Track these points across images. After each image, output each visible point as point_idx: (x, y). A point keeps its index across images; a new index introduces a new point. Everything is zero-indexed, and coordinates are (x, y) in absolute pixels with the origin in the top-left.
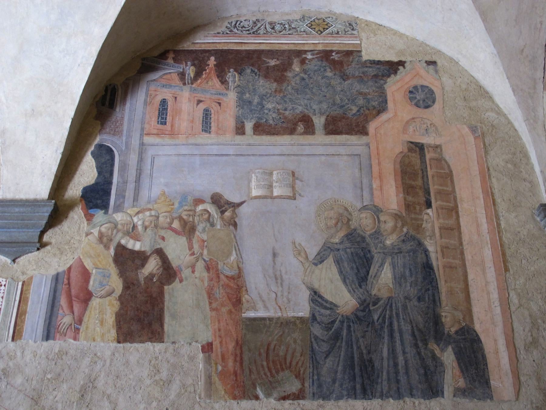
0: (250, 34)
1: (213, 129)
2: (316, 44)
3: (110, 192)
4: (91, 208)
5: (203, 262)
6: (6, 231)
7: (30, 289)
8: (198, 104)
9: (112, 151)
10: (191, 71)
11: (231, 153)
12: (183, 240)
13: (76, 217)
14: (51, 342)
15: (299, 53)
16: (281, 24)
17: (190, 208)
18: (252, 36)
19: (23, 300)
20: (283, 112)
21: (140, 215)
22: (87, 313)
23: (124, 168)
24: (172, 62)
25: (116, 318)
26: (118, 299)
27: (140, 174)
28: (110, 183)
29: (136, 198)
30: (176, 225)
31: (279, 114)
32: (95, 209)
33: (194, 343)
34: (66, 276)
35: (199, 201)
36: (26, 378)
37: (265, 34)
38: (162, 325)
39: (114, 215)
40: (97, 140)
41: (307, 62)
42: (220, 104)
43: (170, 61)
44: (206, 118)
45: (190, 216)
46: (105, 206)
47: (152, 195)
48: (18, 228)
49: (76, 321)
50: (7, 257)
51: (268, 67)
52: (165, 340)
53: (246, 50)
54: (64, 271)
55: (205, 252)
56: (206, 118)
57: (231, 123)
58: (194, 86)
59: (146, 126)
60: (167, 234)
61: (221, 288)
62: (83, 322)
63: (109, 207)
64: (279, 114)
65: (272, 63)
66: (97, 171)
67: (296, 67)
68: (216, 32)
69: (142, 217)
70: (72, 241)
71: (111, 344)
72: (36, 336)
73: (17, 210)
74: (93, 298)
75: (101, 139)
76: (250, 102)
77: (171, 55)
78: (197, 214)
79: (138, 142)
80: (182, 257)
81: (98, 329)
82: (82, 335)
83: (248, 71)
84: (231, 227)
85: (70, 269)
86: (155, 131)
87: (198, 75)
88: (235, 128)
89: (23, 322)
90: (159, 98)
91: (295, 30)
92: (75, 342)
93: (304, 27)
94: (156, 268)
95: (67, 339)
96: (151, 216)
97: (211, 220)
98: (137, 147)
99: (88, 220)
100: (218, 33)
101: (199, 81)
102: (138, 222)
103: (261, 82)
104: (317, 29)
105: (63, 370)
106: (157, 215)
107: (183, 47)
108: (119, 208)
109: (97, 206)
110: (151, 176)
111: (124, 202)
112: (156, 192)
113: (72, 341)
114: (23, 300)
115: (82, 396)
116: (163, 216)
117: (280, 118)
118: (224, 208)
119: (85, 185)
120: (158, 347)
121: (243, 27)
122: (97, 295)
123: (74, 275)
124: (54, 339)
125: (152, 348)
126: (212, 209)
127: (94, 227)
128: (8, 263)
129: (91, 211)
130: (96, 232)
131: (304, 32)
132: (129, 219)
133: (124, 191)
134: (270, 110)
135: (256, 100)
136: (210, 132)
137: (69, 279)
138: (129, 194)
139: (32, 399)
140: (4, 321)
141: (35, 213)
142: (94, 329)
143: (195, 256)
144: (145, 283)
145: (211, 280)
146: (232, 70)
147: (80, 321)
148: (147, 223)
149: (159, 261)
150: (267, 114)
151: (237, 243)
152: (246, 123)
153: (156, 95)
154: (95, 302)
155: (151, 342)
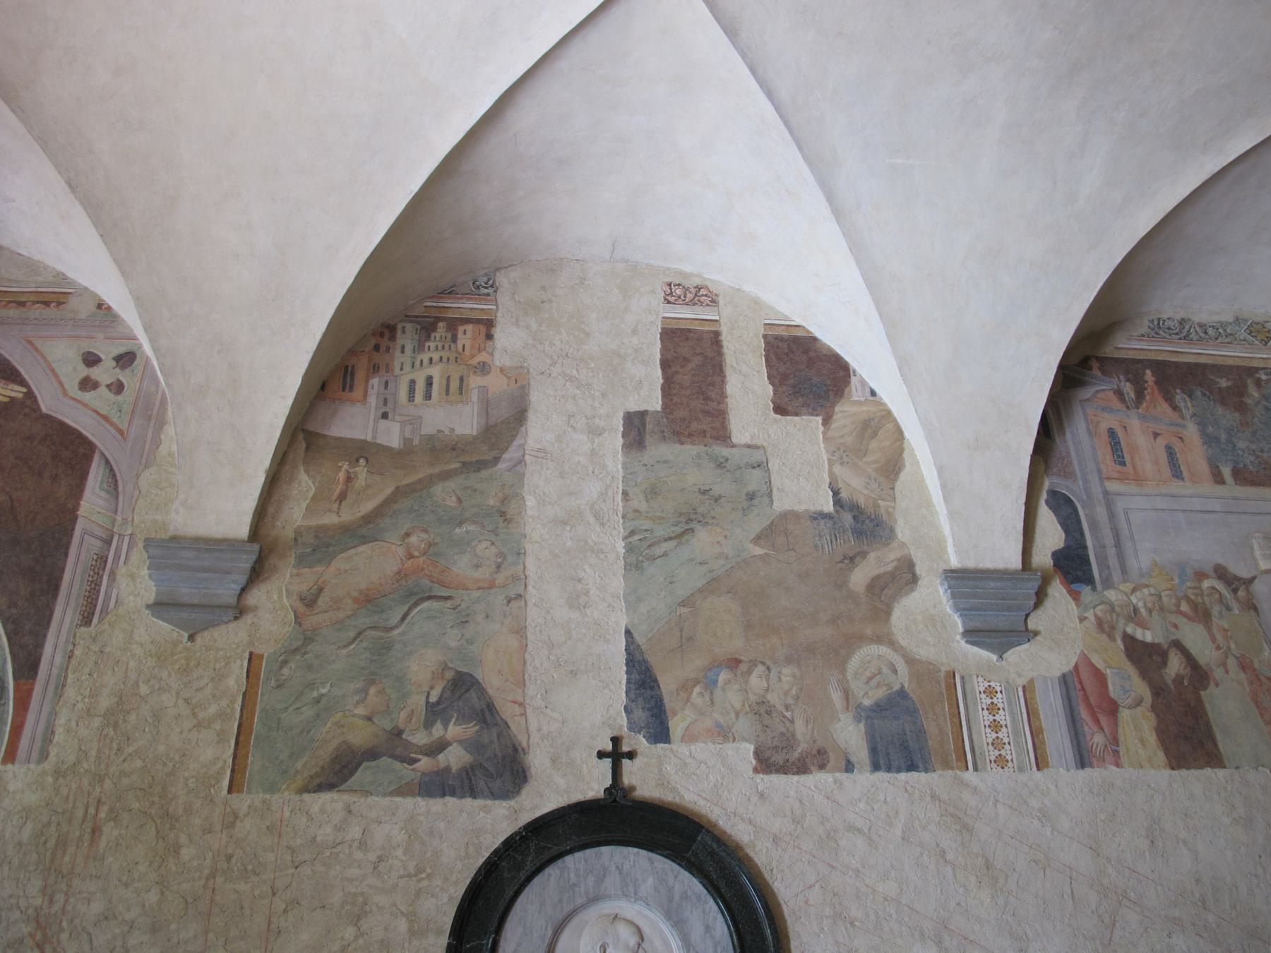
0: (1180, 339)
1: (1185, 474)
2: (1266, 359)
3: (1089, 559)
4: (1072, 583)
5: (1234, 658)
6: (979, 615)
7: (1036, 697)
8: (1155, 438)
9: (1071, 501)
10: (1128, 389)
11: (1218, 510)
12: (1200, 629)
13: (1057, 594)
14: (1088, 770)
15: (1251, 371)
16: (1213, 327)
17: (1193, 585)
18: (1184, 343)
19: (1032, 713)
20: (1260, 454)
21: (1138, 593)
22: (1120, 729)
23: (1094, 526)
24: (1099, 374)
25: (1157, 735)
26: (1150, 709)
27: (1117, 535)
28: (1085, 547)
29: (1124, 570)
30: (1184, 607)
31: (1257, 457)
32: (1079, 584)
33: (1260, 768)
34: (1075, 679)
35: (1200, 575)
36: (1074, 821)
37: (1198, 340)
38: (1215, 745)
39: (1105, 593)
40: (1047, 484)
41: (1263, 384)
42: (1181, 438)
43: (1096, 372)
44: (1172, 459)
45: (1197, 595)
46: (1089, 580)
47: (1142, 566)
48: (998, 611)
49: (1111, 741)
50: (991, 652)
51: (1220, 389)
52: (1227, 766)
53: (1184, 363)
54: (1070, 671)
55: (1233, 646)
56: (1172, 459)
57: (1203, 467)
58: (1140, 411)
59: (1103, 467)
60: (1181, 621)
61: (1266, 693)
62: (1120, 743)
63: (1094, 581)
64: (1257, 457)
65: (1224, 383)
66: (1063, 529)
67: (1253, 392)
68: (1139, 334)
69: (1141, 596)
70: (1065, 629)
71: (1164, 771)
72: (1066, 762)
73: (992, 584)
74: (1121, 709)
75: (1052, 484)
76: (1217, 439)
77: (1095, 365)
78: (1205, 593)
79: (1100, 490)
80: (1207, 652)
81: (1141, 751)
82: (1124, 759)
83: (1198, 393)
84: (1252, 612)
85: (1076, 667)
86: (1115, 475)
87: (1140, 395)
88: (1211, 475)
89: (1043, 743)
90: (1104, 427)
91: (1232, 337)
92: (1118, 770)
93: (1243, 335)
94: (1182, 668)
95: (1108, 766)
96: (1152, 595)
97: (1224, 601)
98: (1101, 496)
99: (1075, 599)
100: (1143, 336)
101: (1144, 405)
102: (1137, 602)
103: (1220, 410)
104: (1259, 338)
105: (1116, 808)
106: (1158, 593)
107: (1105, 353)
108: (1108, 584)
109: (1077, 580)
110: (1132, 537)
111: (1110, 574)
112: (1145, 561)
113: (1114, 768)
114: (1032, 713)
115: (1152, 842)
116: (1166, 596)
117: (1259, 462)
118: (1234, 586)
119: (1054, 550)
120: (1221, 773)
121: (1169, 328)
122: (1125, 704)
123: (1085, 675)
124: (1092, 766)
125: (1214, 775)
126: (1220, 586)
127: (1086, 609)
128: (993, 660)
129: (1075, 586)
130: (1090, 614)
131: (1245, 340)
132: (1125, 598)
133: (1106, 558)
134: (1243, 451)
135: (1223, 437)
136: (1183, 479)
137: (1081, 683)
138: (1113, 562)
139: (1091, 848)
140: (1018, 743)
141: (1016, 589)
142: (1137, 752)
143: (1222, 651)
144: (1175, 687)
145: (1251, 683)
146: (1178, 391)
147: (1116, 741)
148: (1150, 605)
149: (1182, 657)
150: (1242, 456)
151: (1264, 632)
152: (1221, 468)
153: (1099, 422)
154: (1124, 714)
155: (1211, 767)
